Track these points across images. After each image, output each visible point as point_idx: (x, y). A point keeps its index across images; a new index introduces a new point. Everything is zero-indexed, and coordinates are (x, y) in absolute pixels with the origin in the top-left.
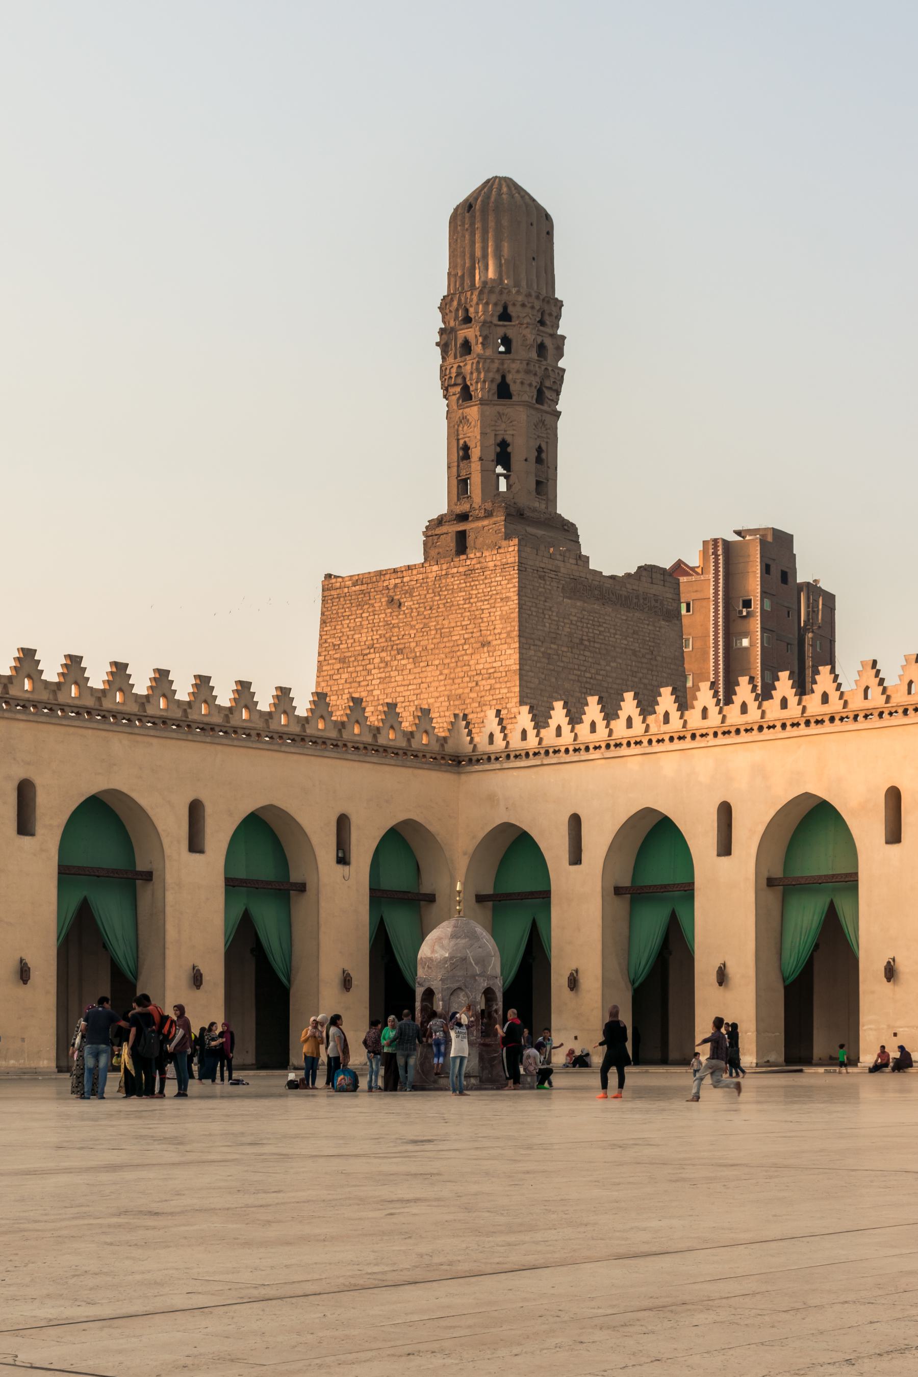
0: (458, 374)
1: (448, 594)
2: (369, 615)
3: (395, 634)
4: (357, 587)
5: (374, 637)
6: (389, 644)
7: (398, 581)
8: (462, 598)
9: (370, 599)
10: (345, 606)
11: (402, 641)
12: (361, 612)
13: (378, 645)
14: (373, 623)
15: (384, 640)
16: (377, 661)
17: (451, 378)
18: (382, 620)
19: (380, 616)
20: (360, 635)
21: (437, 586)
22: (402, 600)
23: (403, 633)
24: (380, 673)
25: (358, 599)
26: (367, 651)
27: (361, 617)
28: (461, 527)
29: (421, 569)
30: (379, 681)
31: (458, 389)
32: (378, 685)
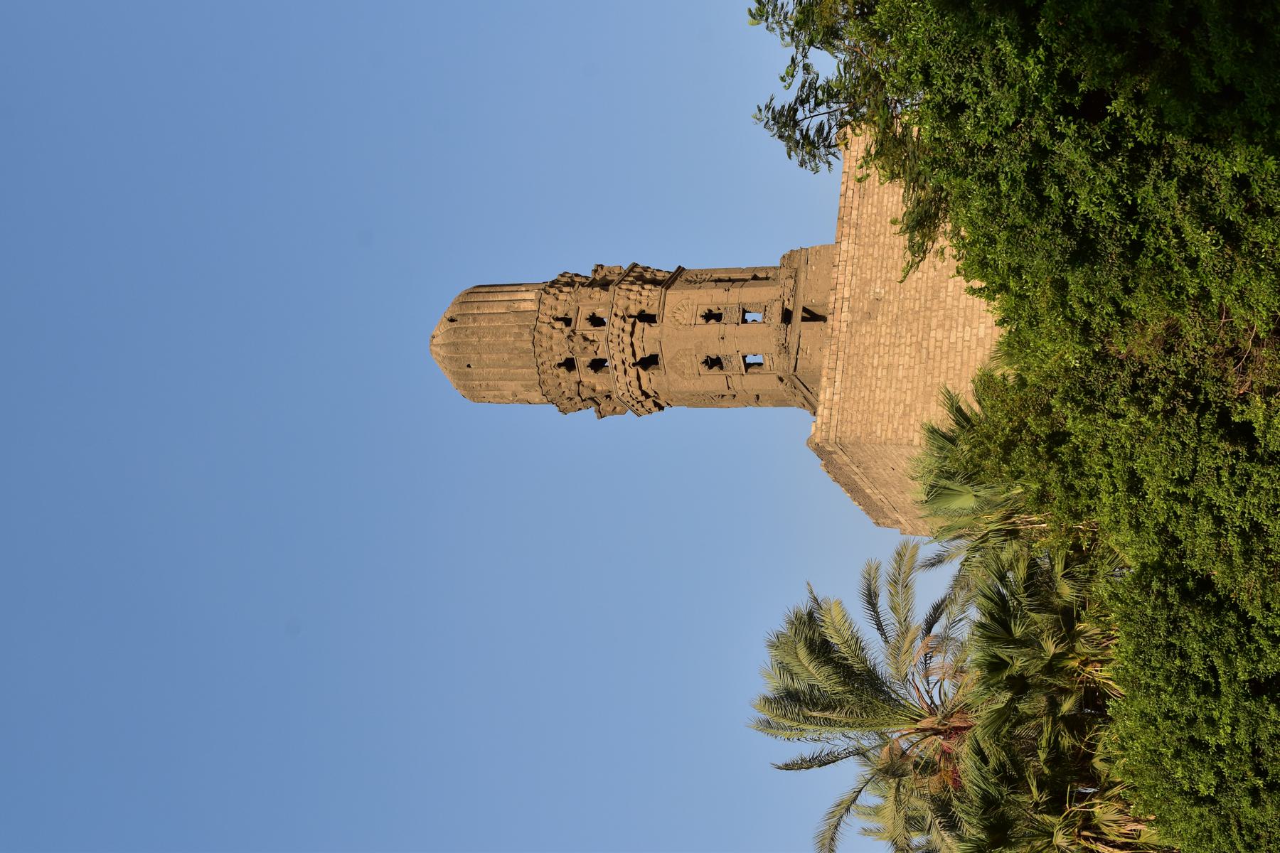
0: (623, 318)
1: (880, 222)
2: (878, 353)
3: (912, 304)
4: (838, 377)
5: (908, 341)
6: (922, 314)
7: (845, 309)
8: (891, 199)
9: (857, 354)
10: (856, 399)
11: (923, 293)
12: (870, 367)
13: (920, 335)
14: (889, 346)
15: (915, 324)
16: (940, 334)
17: (623, 330)
18: (888, 331)
19: (883, 333)
20: (901, 367)
21: (867, 240)
22: (872, 297)
23: (913, 292)
24: (957, 327)
25: (852, 376)
26: (924, 351)
27: (877, 368)
28: (798, 315)
29: (840, 268)
30: (967, 328)
31: (639, 325)
32: (972, 329)
